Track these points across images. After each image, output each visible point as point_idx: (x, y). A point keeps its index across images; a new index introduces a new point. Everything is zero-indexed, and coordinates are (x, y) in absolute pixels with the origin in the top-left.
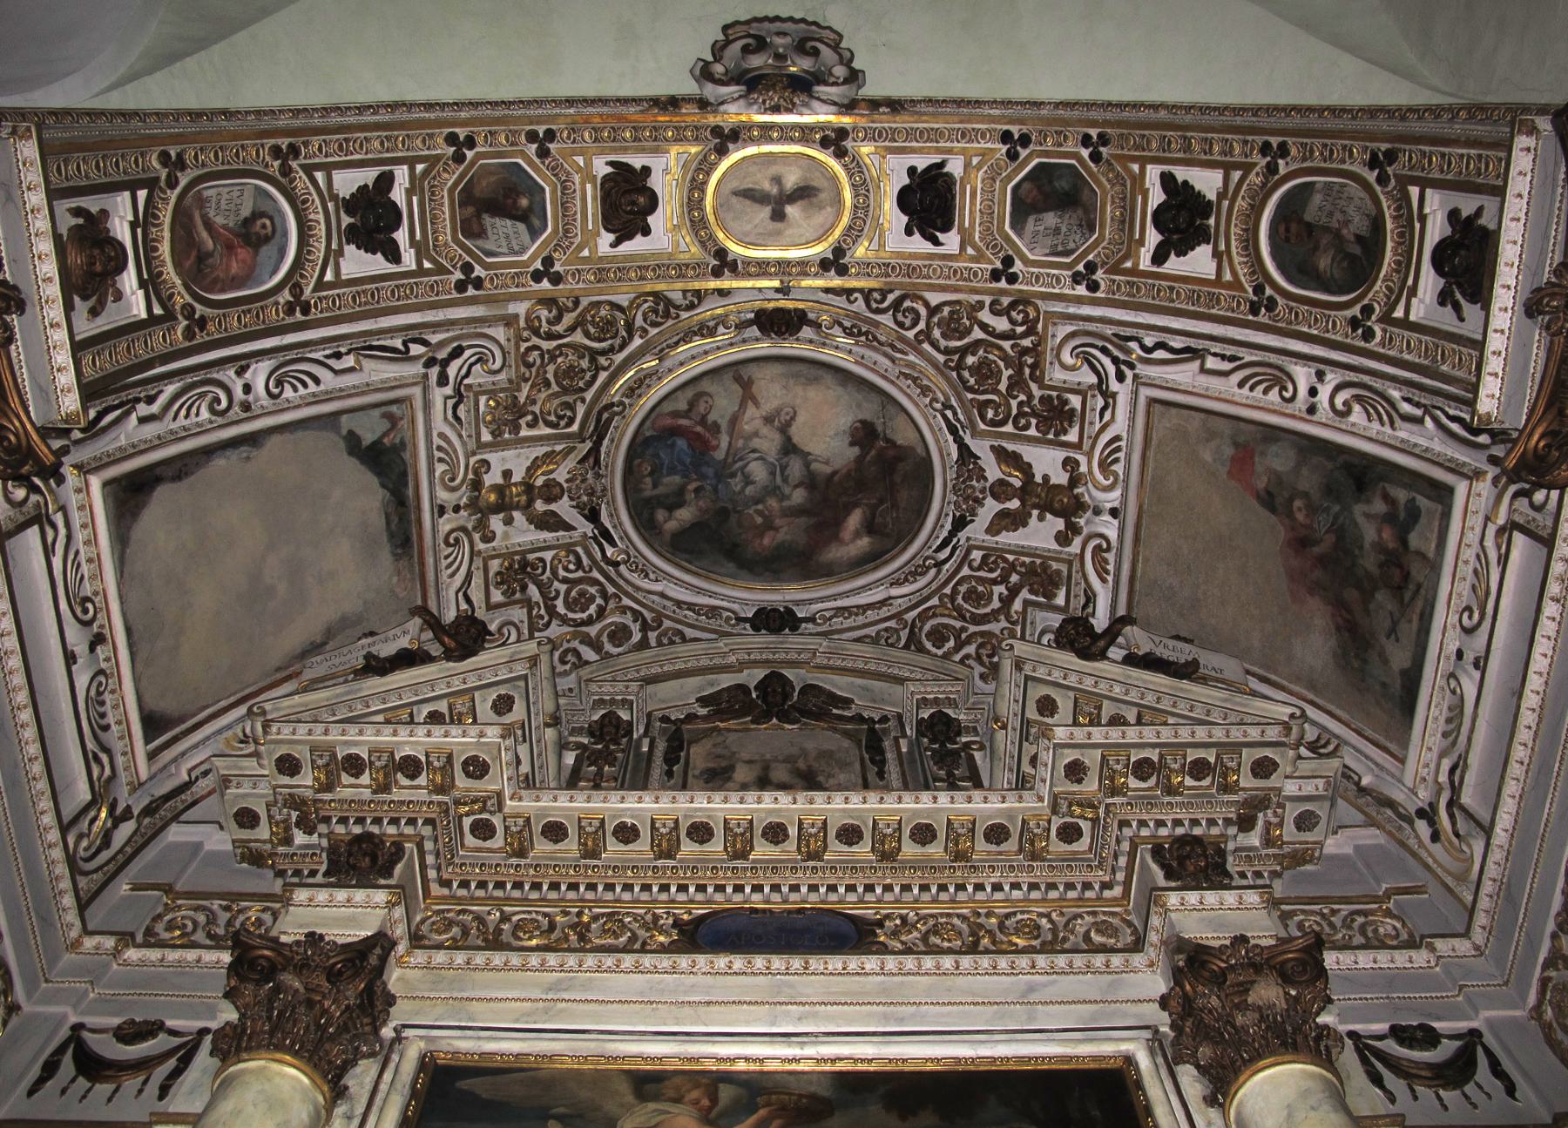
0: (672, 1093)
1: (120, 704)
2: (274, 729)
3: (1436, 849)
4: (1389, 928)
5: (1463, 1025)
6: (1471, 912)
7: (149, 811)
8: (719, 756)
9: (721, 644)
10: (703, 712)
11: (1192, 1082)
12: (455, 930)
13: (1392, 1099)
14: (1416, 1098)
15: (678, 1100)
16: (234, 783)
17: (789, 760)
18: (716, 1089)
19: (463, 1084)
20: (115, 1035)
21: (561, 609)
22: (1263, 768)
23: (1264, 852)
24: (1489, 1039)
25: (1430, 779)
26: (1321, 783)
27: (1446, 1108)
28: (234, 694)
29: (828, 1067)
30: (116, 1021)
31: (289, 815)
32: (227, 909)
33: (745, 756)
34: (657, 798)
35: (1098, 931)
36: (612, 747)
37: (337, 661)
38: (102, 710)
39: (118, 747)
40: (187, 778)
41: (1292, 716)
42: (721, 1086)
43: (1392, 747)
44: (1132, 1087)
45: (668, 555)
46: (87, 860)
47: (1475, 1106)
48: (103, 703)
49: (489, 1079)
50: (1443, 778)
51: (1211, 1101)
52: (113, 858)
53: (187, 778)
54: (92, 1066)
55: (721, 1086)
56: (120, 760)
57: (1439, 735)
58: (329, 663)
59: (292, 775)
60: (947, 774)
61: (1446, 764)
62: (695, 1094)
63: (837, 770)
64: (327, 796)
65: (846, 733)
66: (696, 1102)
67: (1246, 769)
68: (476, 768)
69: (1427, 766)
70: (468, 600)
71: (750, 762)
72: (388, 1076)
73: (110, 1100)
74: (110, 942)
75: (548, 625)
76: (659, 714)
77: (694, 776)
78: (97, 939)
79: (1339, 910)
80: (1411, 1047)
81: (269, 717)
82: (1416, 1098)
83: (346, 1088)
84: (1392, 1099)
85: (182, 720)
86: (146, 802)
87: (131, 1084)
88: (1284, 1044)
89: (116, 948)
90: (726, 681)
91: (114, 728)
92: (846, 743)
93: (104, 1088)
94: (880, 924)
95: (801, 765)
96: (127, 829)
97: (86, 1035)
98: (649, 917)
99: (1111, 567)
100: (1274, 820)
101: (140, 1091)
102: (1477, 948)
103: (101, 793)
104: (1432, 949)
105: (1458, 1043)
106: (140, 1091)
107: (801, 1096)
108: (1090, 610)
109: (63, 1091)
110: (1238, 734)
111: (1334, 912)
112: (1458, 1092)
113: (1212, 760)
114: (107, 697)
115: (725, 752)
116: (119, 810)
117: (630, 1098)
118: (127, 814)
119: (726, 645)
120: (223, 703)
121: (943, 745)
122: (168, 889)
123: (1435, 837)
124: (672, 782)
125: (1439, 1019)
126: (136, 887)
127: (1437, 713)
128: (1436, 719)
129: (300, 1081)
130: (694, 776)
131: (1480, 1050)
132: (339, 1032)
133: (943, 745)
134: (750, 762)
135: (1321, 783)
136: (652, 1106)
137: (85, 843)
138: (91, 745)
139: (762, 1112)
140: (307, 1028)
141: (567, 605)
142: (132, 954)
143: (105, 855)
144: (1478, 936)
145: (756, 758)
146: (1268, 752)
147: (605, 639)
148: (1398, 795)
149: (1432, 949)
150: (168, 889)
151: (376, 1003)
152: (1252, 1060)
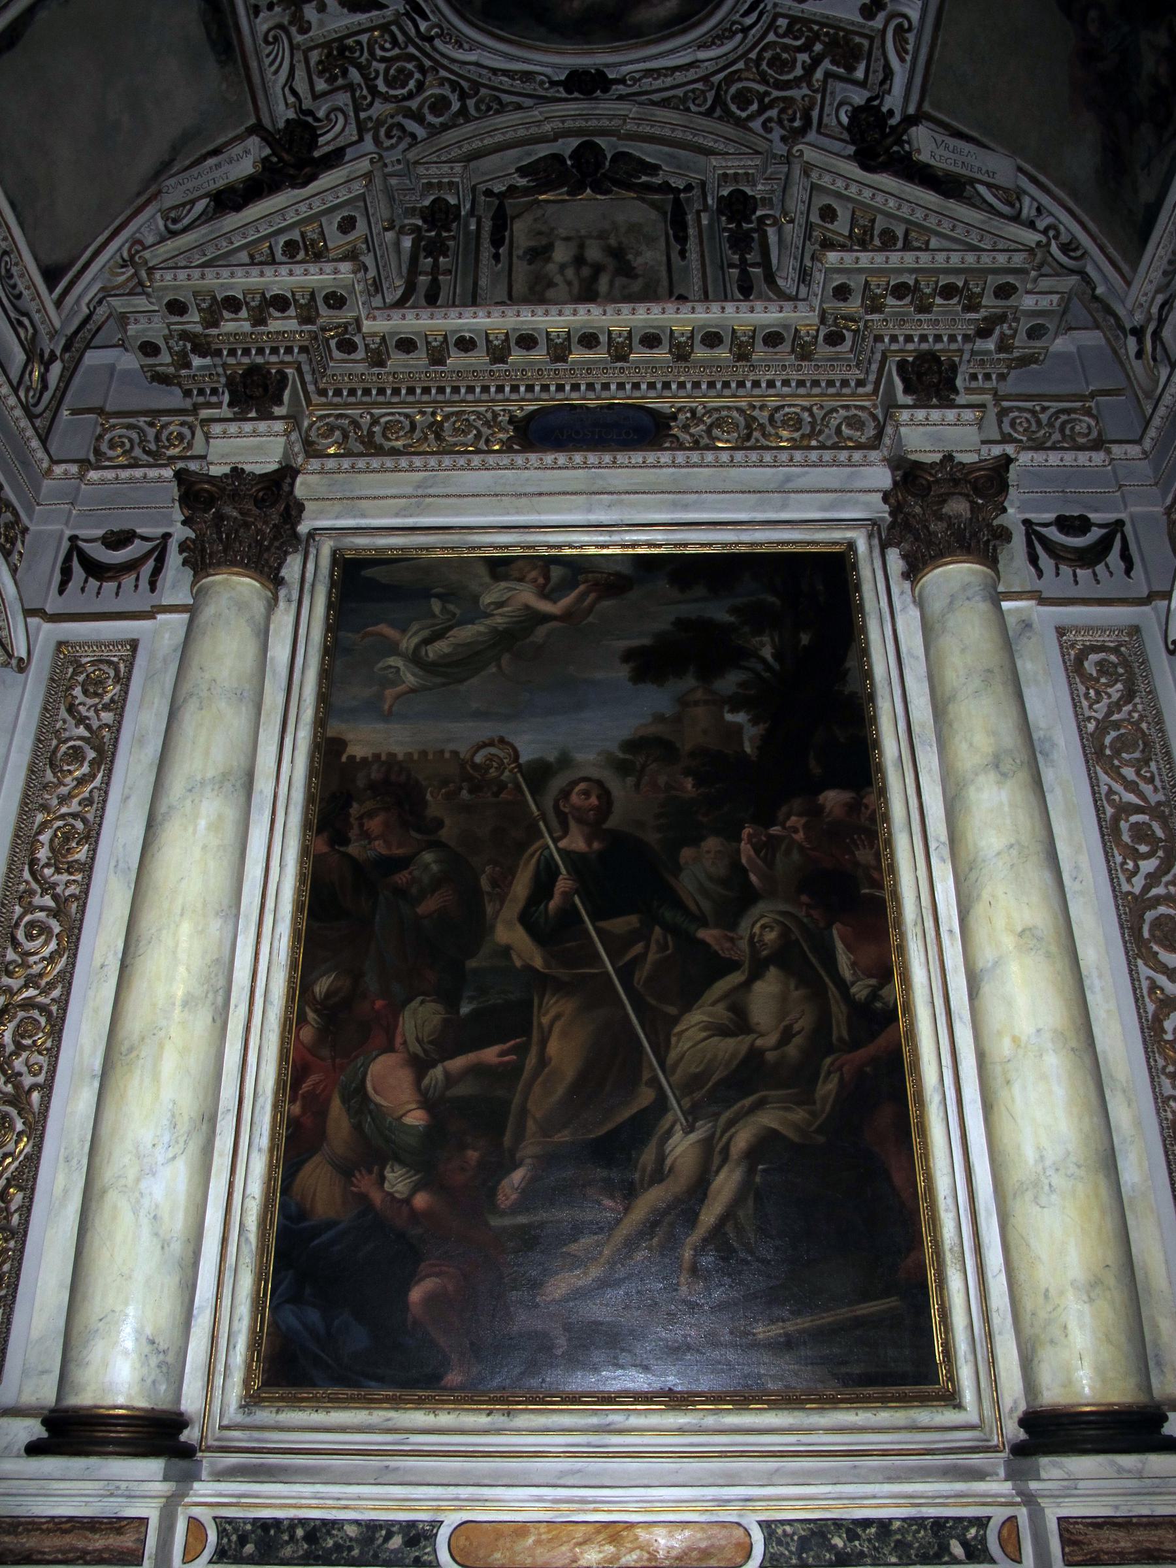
0: (516, 574)
1: (24, 274)
2: (158, 276)
3: (1137, 365)
4: (1084, 425)
5: (1111, 517)
6: (1148, 423)
7: (67, 348)
8: (540, 233)
9: (536, 113)
10: (522, 182)
11: (895, 560)
12: (337, 433)
13: (1040, 573)
14: (1058, 574)
15: (521, 580)
16: (132, 320)
17: (602, 236)
18: (549, 571)
19: (368, 573)
20: (103, 543)
21: (382, 88)
22: (1005, 291)
23: (996, 356)
24: (1128, 529)
25: (1146, 305)
26: (1055, 298)
27: (1076, 582)
28: (106, 228)
29: (630, 551)
30: (100, 532)
31: (185, 345)
32: (151, 425)
33: (563, 232)
34: (489, 313)
35: (849, 425)
36: (445, 234)
37: (190, 185)
38: (12, 282)
39: (33, 307)
40: (87, 311)
41: (1039, 244)
42: (552, 567)
43: (1125, 268)
44: (849, 567)
45: (481, 24)
46: (36, 405)
47: (1098, 582)
48: (11, 277)
49: (384, 568)
50: (1154, 310)
51: (906, 576)
52: (54, 395)
53: (87, 311)
54: (96, 570)
55: (552, 567)
56: (36, 317)
57: (1160, 272)
58: (184, 188)
59: (181, 314)
60: (740, 259)
61: (1160, 299)
62: (533, 574)
63: (644, 247)
64: (213, 331)
65: (653, 205)
66: (535, 580)
67: (989, 291)
68: (336, 301)
69: (1146, 294)
70: (294, 93)
71: (567, 239)
72: (310, 566)
73: (117, 594)
74: (74, 469)
75: (371, 105)
76: (482, 187)
77: (518, 257)
78: (63, 467)
79: (1048, 408)
80: (1067, 534)
81: (150, 265)
82: (1058, 574)
83: (283, 578)
84: (1040, 573)
86: (63, 342)
87: (128, 580)
88: (961, 547)
89: (80, 472)
90: (543, 150)
91: (26, 293)
92: (654, 215)
93: (110, 586)
94: (674, 417)
95: (613, 242)
96: (56, 368)
97: (80, 543)
98: (489, 415)
99: (910, 47)
100: (1008, 332)
101: (136, 587)
102: (1144, 452)
103: (32, 351)
104: (1108, 451)
105: (1104, 531)
106: (136, 587)
107: (610, 574)
108: (887, 87)
109: (83, 589)
110: (987, 260)
111: (1044, 409)
112: (1090, 571)
113: (960, 284)
114: (14, 270)
117: (487, 579)
118: (53, 357)
119: (541, 113)
120: (101, 239)
121: (739, 225)
122: (100, 411)
123: (1139, 354)
124: (500, 266)
125: (1096, 511)
126: (74, 412)
127: (1163, 253)
128: (1161, 258)
129: (254, 586)
130: (518, 257)
131: (1119, 536)
132: (271, 544)
133: (739, 225)
134: (567, 239)
135: (1055, 298)
136: (503, 584)
137: (31, 394)
138: (13, 315)
139: (582, 588)
140: (250, 546)
141: (390, 83)
142: (93, 475)
143: (47, 396)
144: (1147, 444)
146: (1010, 279)
147: (426, 110)
148: (1121, 312)
149: (1108, 451)
150: (100, 411)
151: (293, 511)
152: (933, 558)
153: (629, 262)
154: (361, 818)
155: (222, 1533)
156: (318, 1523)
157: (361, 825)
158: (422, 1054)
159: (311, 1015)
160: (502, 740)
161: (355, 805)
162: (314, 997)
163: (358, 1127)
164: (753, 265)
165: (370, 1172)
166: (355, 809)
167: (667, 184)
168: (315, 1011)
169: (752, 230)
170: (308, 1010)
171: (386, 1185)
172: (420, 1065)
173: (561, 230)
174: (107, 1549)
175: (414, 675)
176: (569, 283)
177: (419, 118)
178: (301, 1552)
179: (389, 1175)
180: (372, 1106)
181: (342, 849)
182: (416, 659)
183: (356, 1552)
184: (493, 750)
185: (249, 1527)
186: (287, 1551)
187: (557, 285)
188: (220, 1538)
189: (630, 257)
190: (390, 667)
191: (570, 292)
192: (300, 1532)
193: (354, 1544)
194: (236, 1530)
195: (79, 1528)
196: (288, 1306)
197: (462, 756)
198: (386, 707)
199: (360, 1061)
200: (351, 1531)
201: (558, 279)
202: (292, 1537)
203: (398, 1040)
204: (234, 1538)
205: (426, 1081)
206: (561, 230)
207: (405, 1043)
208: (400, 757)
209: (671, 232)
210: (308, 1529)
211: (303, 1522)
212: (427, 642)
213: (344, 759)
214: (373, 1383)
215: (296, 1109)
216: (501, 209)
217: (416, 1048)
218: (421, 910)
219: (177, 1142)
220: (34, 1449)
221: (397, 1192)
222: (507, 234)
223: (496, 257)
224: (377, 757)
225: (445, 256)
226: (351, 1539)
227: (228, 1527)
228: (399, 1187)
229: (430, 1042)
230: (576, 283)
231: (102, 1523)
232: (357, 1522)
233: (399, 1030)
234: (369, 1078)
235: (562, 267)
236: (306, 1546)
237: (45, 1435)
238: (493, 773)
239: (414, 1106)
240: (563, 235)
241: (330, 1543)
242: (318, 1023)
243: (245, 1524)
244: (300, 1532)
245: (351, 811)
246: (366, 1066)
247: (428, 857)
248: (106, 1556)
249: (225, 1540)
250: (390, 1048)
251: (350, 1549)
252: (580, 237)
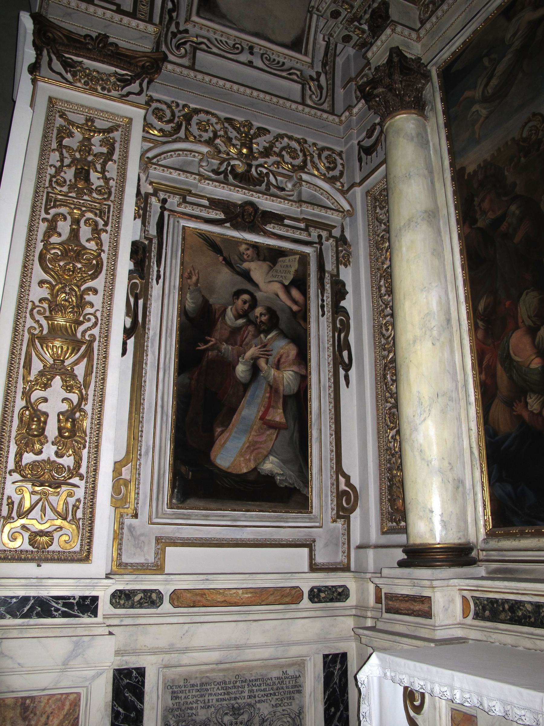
1: (279, 54)
2: (321, 9)
7: (324, 65)
16: (333, 33)
31: (354, 25)
38: (276, 62)
39: (293, 64)
40: (325, 43)
48: (274, 60)
53: (325, 43)
56: (298, 66)
59: (340, 15)
64: (354, 10)
73: (377, 157)
74: (347, 113)
78: (344, 115)
81: (316, 6)
85: (303, 31)
86: (320, 64)
89: (350, 114)
91: (285, 61)
96: (323, 79)
97: (362, 143)
103: (303, 81)
109: (367, 164)
114: (273, 57)
116: (315, 76)
118: (318, 74)
126: (344, 87)
136: (514, 20)
137: (314, 97)
138: (284, 74)
142: (355, 110)
143: (324, 92)
154: (480, 204)
155: (475, 604)
156: (513, 602)
157: (481, 208)
158: (532, 324)
159: (480, 323)
160: (534, 115)
161: (476, 199)
162: (480, 313)
163: (511, 378)
165: (520, 401)
166: (476, 201)
168: (481, 320)
170: (478, 321)
171: (529, 407)
172: (532, 332)
174: (420, 610)
175: (485, 108)
178: (508, 617)
179: (529, 401)
180: (515, 364)
181: (475, 226)
182: (485, 100)
183: (532, 620)
184: (530, 124)
185: (485, 602)
186: (502, 616)
188: (475, 607)
190: (474, 112)
192: (506, 606)
193: (531, 615)
194: (481, 603)
195: (410, 600)
196: (498, 484)
197: (516, 139)
198: (477, 136)
199: (505, 339)
200: (529, 607)
202: (504, 608)
203: (520, 320)
204: (480, 607)
205: (537, 340)
207: (523, 321)
208: (489, 159)
210: (510, 605)
211: (507, 601)
212: (486, 85)
213: (466, 177)
214: (539, 523)
215: (483, 377)
217: (529, 322)
218: (516, 241)
219: (425, 411)
220: (402, 564)
221: (534, 409)
224: (479, 166)
226: (529, 612)
227: (478, 602)
228: (535, 406)
229: (535, 316)
231: (417, 598)
232: (530, 603)
233: (519, 315)
234: (511, 348)
236: (510, 614)
237: (406, 557)
238: (534, 137)
239: (534, 357)
241: (520, 613)
242: (483, 326)
243: (484, 600)
244: (506, 606)
245: (475, 203)
246: (508, 342)
247: (513, 208)
248: (420, 613)
249: (477, 608)
250: (517, 328)
251: (530, 617)
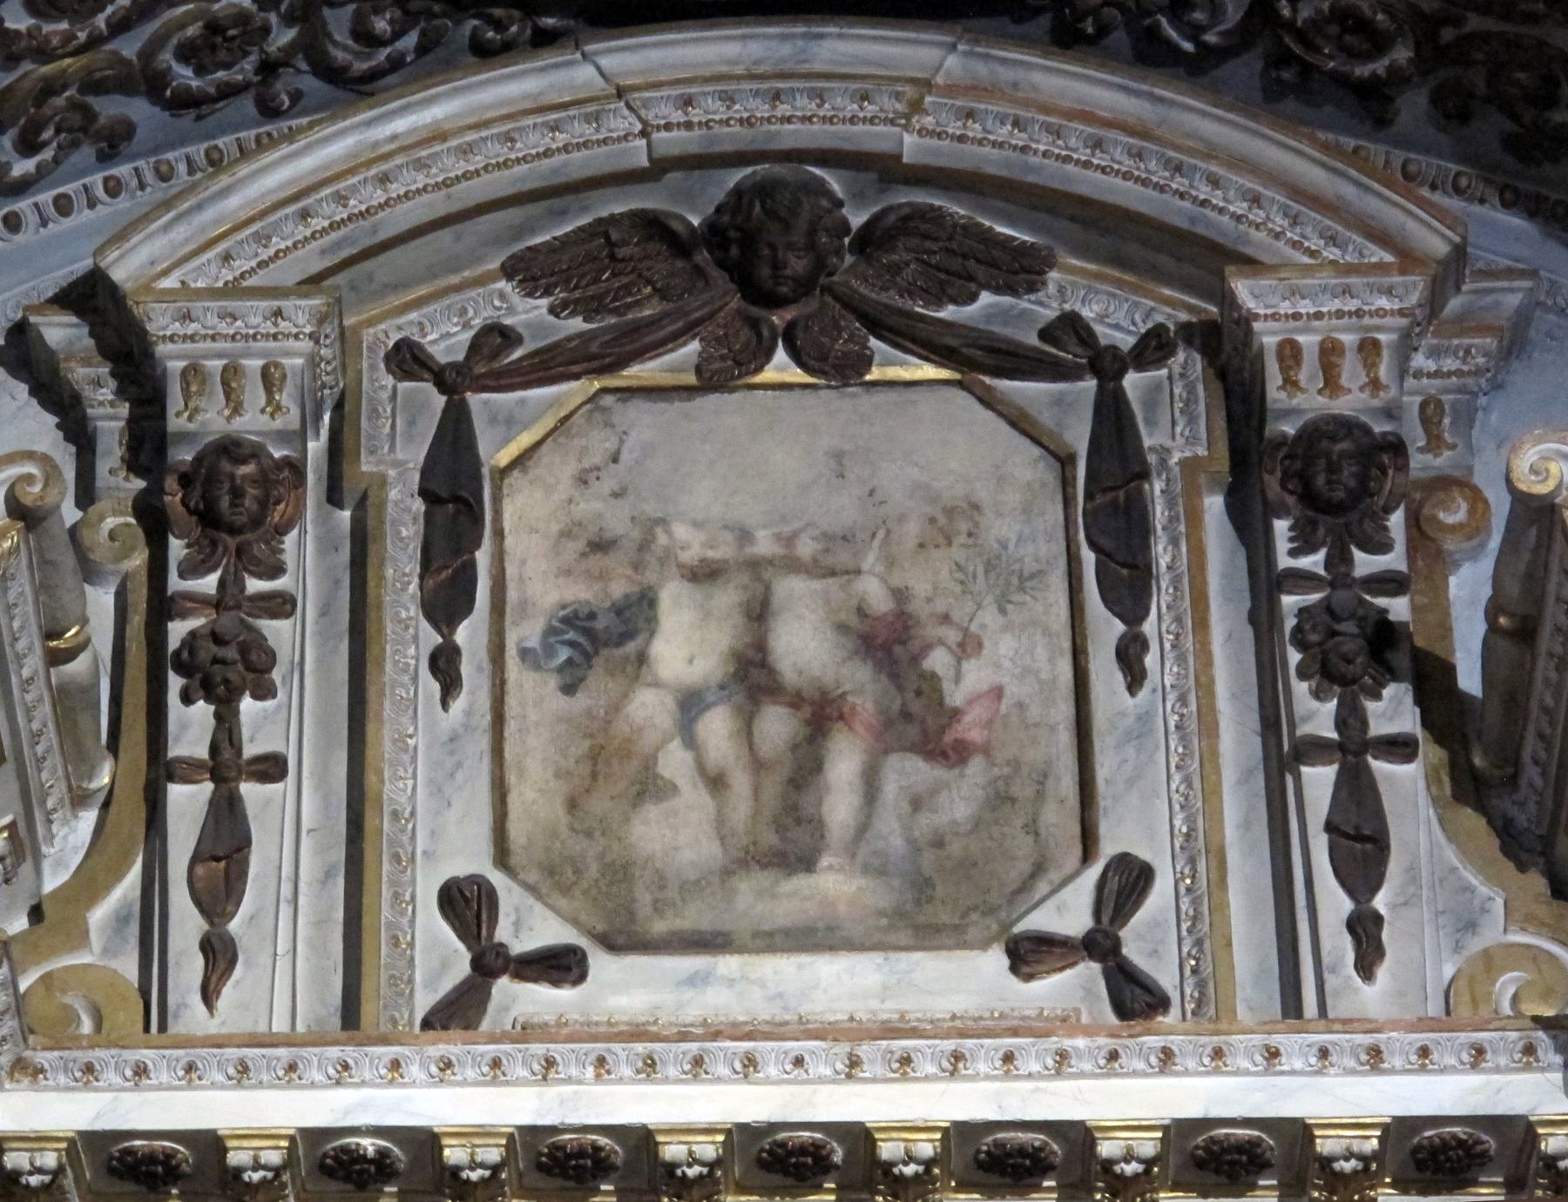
8: (601, 546)
33: (690, 542)
36: (254, 585)
63: (989, 617)
65: (1020, 422)
71: (704, 574)
77: (524, 653)
95: (874, 592)
115: (617, 521)
121: (1339, 560)
124: (459, 705)
133: (1339, 560)
134: (704, 574)
145: (724, 551)
147: (167, 57)
153: (933, 678)
164: (1399, 748)
167: (1070, 327)
169: (1391, 583)
173: (681, 531)
176: (716, 783)
177: (153, 85)
187: (672, 789)
189: (938, 661)
191: (720, 822)
201: (675, 762)
206: (681, 531)
209: (1089, 558)
216: (454, 429)
222: (482, 557)
223: (445, 665)
225: (264, 691)
230: (741, 783)
235: (691, 704)
240: (690, 556)
252: (755, 565)
